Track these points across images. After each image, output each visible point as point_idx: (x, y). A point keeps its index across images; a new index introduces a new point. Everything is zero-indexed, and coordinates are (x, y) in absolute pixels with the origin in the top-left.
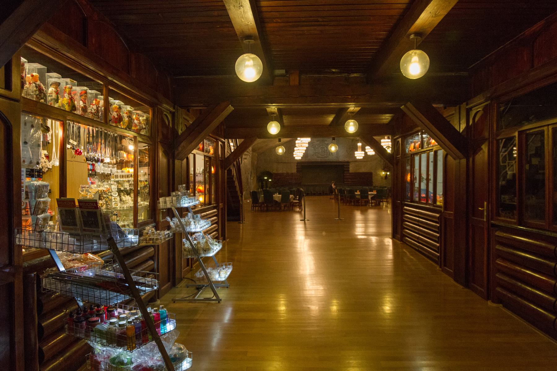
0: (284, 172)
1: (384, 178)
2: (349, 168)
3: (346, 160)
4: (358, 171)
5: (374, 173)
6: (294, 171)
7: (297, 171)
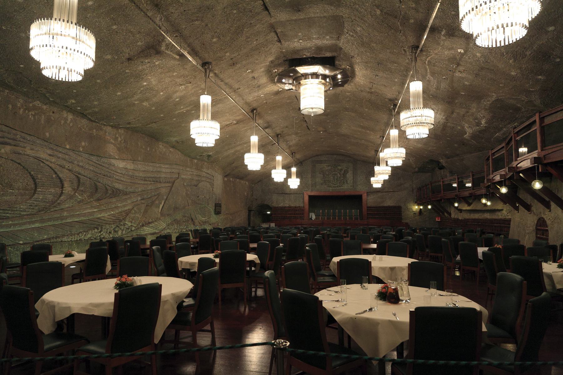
4: (382, 205)
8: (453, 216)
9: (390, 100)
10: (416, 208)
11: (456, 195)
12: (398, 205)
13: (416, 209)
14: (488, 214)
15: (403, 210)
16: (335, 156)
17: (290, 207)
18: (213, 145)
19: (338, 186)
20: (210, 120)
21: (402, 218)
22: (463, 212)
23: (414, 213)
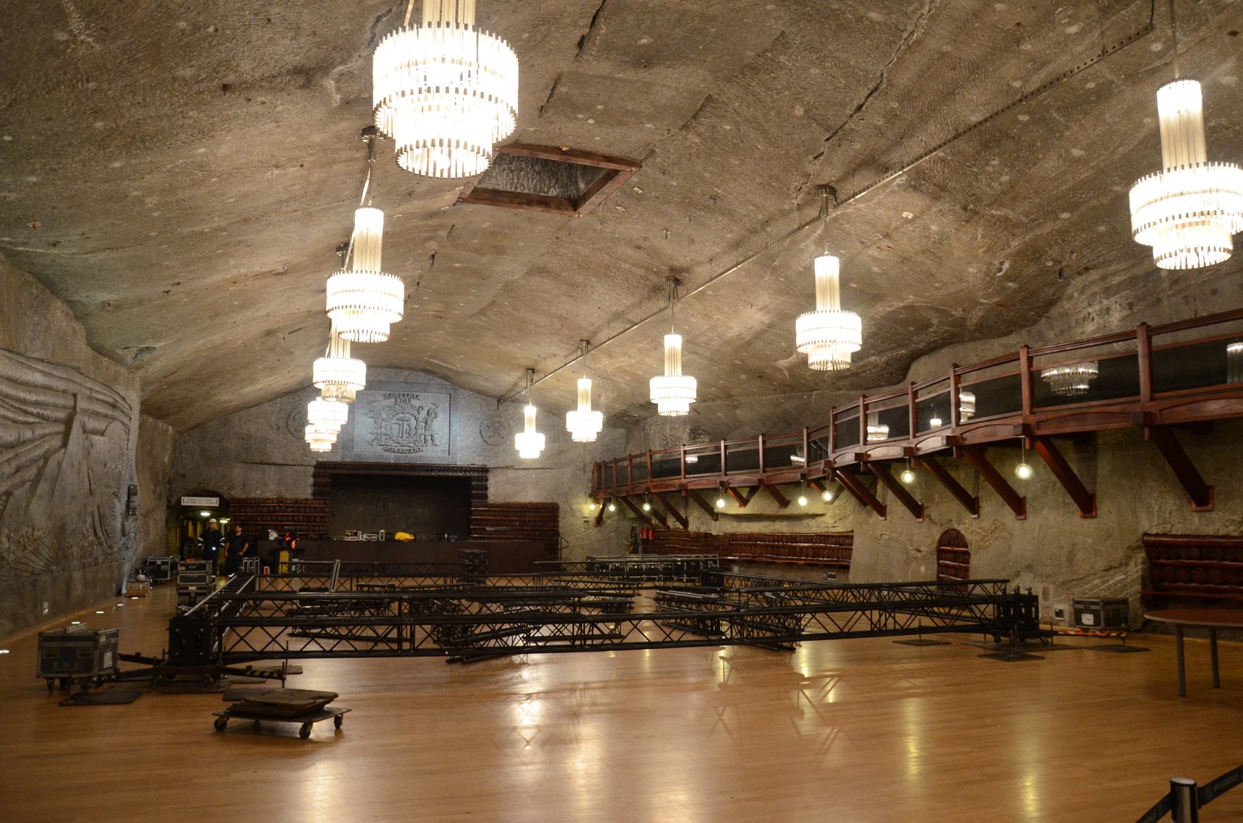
0: (268, 495)
1: (592, 521)
2: (486, 488)
3: (478, 462)
5: (562, 507)
6: (304, 490)
7: (314, 494)
8: (692, 527)
9: (672, 269)
10: (591, 509)
11: (722, 483)
12: (550, 501)
13: (591, 511)
14: (785, 523)
15: (561, 514)
16: (407, 373)
17: (280, 500)
18: (385, 339)
19: (412, 451)
20: (378, 273)
21: (560, 531)
22: (719, 518)
23: (585, 522)
